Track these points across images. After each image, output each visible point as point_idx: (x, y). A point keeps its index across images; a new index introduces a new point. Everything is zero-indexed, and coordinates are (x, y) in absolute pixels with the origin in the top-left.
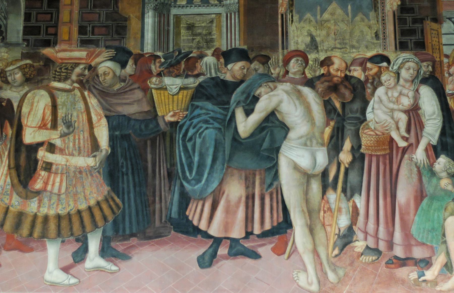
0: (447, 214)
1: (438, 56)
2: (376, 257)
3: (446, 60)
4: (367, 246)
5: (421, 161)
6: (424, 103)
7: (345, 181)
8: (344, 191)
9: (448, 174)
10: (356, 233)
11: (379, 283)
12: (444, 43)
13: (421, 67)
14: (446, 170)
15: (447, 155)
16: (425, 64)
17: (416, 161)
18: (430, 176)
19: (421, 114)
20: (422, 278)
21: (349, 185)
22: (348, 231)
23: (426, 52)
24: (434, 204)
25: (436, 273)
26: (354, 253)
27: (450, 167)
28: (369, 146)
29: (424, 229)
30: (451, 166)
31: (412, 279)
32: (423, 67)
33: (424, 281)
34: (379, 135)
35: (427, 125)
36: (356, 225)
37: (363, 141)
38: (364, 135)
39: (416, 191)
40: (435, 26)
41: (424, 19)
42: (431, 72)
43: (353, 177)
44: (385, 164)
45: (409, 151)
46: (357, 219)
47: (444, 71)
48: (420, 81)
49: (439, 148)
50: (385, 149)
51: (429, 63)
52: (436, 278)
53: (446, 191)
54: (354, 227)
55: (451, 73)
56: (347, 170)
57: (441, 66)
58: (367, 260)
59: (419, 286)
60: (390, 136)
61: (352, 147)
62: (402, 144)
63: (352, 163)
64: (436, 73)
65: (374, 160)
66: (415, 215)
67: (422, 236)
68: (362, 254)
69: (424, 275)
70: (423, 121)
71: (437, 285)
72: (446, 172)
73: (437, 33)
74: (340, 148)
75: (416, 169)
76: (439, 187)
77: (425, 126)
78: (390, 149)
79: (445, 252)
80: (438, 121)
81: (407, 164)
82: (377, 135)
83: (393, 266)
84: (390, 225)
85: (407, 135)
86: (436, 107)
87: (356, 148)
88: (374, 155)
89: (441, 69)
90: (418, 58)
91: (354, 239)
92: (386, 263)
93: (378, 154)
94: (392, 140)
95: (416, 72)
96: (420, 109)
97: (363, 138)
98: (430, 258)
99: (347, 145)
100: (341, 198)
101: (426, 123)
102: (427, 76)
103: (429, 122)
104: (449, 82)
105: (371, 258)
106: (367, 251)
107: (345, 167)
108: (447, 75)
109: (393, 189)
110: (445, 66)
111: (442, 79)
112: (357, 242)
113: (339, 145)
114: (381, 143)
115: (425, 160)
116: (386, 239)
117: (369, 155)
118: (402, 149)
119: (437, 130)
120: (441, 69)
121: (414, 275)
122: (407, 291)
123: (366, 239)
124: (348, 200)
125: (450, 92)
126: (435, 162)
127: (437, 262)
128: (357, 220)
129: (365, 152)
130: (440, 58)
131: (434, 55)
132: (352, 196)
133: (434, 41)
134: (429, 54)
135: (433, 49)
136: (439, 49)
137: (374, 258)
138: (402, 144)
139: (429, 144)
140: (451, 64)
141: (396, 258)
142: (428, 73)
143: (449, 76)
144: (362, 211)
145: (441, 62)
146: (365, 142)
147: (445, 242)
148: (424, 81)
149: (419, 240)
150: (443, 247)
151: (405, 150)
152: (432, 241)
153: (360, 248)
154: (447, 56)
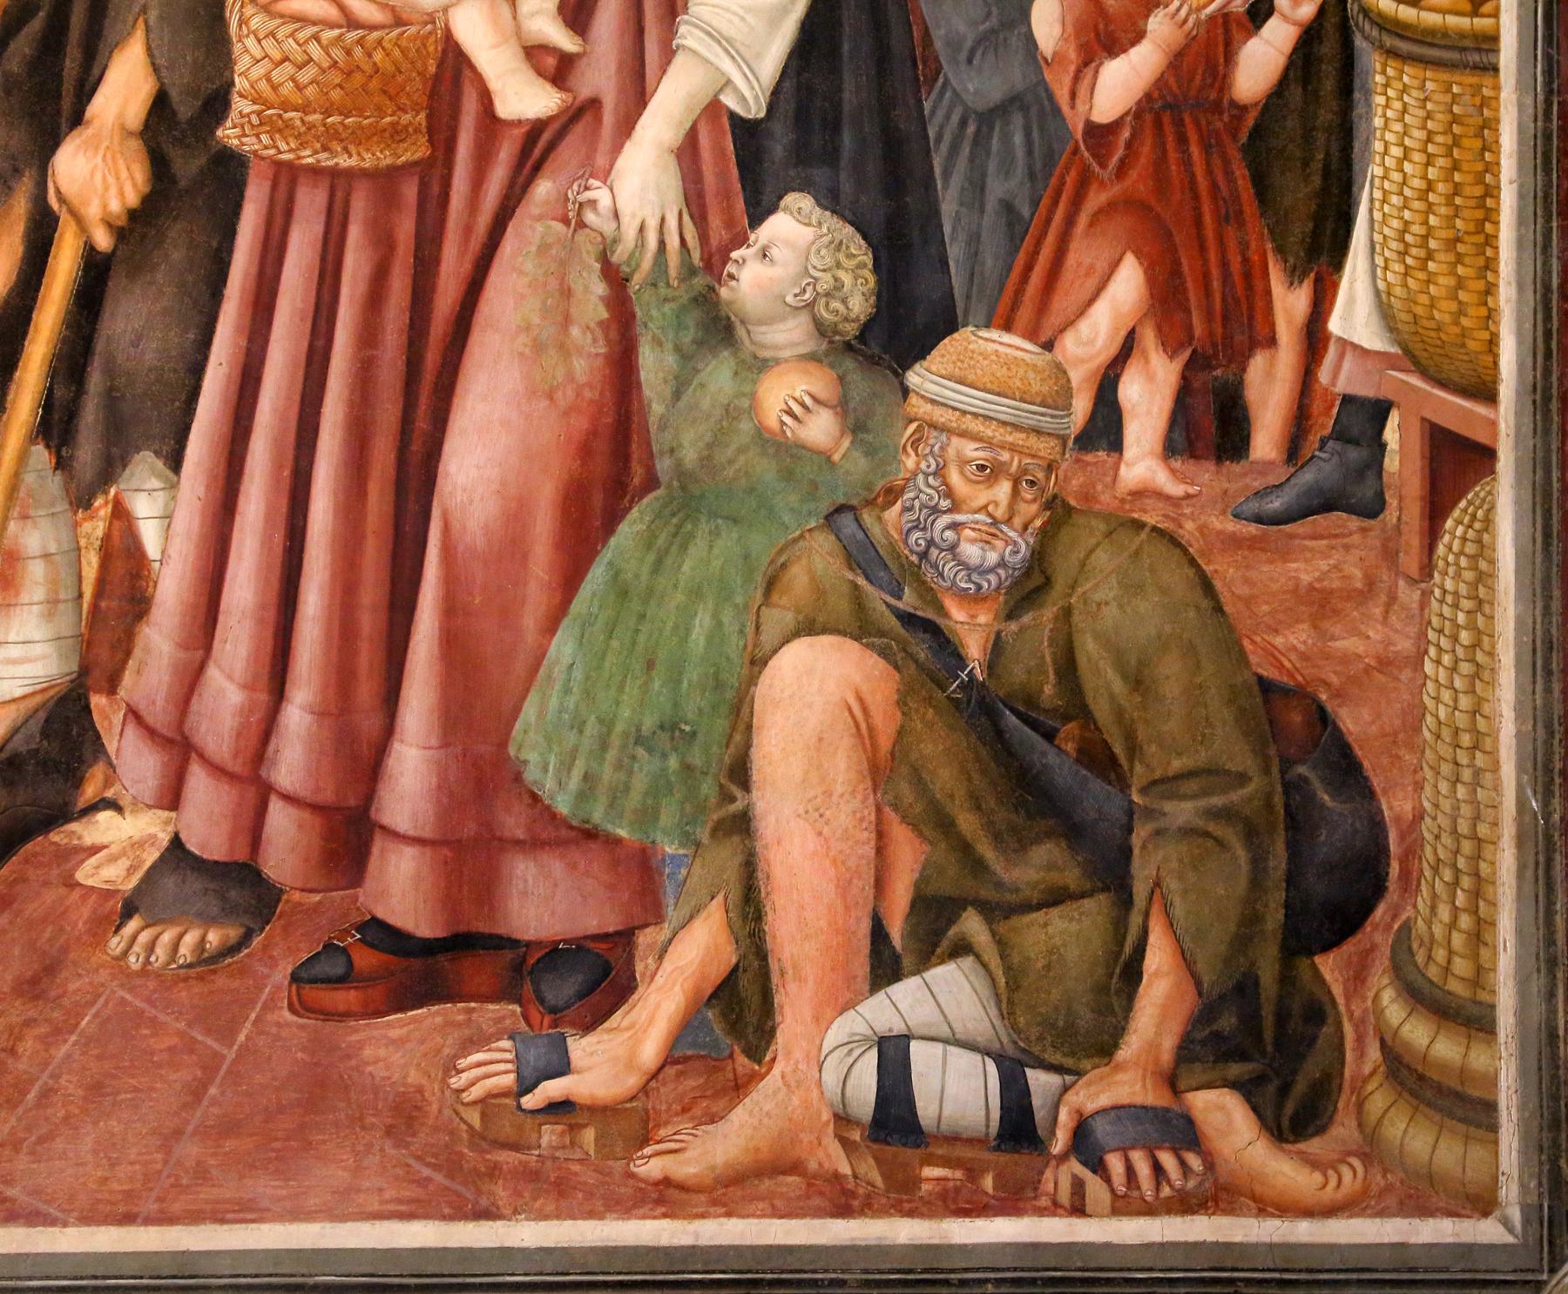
0: (778, 618)
2: (234, 933)
4: (176, 842)
5: (642, 229)
7: (73, 360)
8: (55, 426)
10: (111, 746)
11: (229, 1127)
14: (810, 305)
15: (831, 201)
17: (608, 228)
18: (699, 343)
20: (552, 1089)
21: (95, 381)
22: (45, 733)
24: (697, 549)
25: (650, 1051)
26: (76, 894)
27: (838, 285)
28: (286, 106)
29: (607, 724)
30: (847, 279)
31: (476, 1092)
33: (560, 1108)
34: (373, 28)
36: (112, 687)
37: (242, 63)
38: (255, 23)
39: (585, 451)
43: (136, 324)
44: (383, 245)
45: (569, 151)
46: (125, 646)
49: (779, 147)
50: (397, 134)
52: (644, 1089)
53: (787, 452)
54: (97, 701)
56: (96, 274)
58: (161, 953)
59: (515, 1147)
60: (448, 36)
61: (160, 104)
62: (524, 98)
63: (139, 225)
65: (310, 205)
66: (551, 626)
67: (586, 777)
68: (129, 911)
69: (563, 1068)
71: (645, 1141)
72: (804, 319)
74: (67, 103)
75: (600, 288)
76: (745, 426)
78: (431, 131)
79: (736, 894)
81: (543, 249)
82: (352, 22)
83: (345, 998)
84: (367, 691)
85: (565, 41)
87: (185, 109)
88: (315, 171)
91: (90, 791)
92: (295, 978)
93: (344, 162)
94: (454, 65)
97: (250, 42)
98: (624, 938)
99: (125, 87)
100: (29, 478)
105: (190, 939)
106: (170, 883)
107: (90, 251)
109: (422, 423)
112: (104, 816)
113: (58, 77)
114: (374, 84)
115: (672, 223)
116: (328, 796)
117: (279, 165)
118: (518, 132)
121: (489, 1070)
122: (424, 1182)
123: (172, 797)
124: (82, 501)
126: (741, 241)
127: (668, 965)
128: (128, 654)
129: (249, 145)
132: (109, 470)
137: (214, 938)
138: (524, 98)
141: (380, 933)
144: (172, 587)
146: (258, 71)
147: (742, 825)
149: (563, 806)
150: (726, 858)
151: (537, 146)
152: (646, 816)
153: (124, 863)
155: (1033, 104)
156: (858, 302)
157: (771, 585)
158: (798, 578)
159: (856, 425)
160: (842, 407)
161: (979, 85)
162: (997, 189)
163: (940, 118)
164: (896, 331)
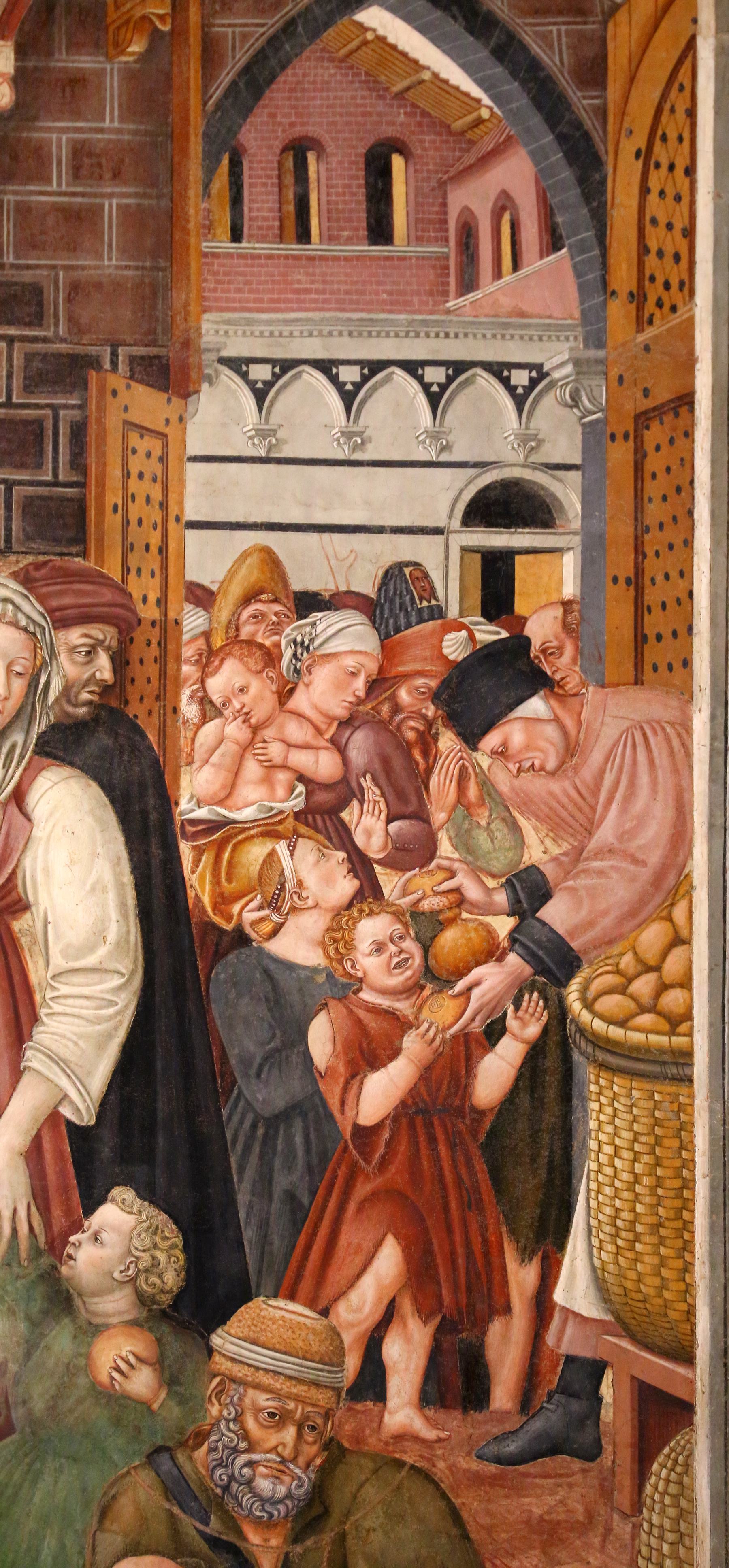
1: (152, 597)
3: (193, 621)
6: (47, 871)
9: (142, 1299)
12: (191, 515)
13: (53, 654)
14: (133, 1280)
15: (148, 1193)
16: (75, 636)
18: (45, 1313)
19: (24, 941)
23: (90, 564)
30: (162, 1257)
32: (63, 658)
35: (56, 1008)
40: (146, 403)
41: (94, 363)
42: (106, 690)
47: (178, 684)
48: (40, 736)
51: (97, 631)
55: (217, 699)
57: (162, 660)
64: (133, 694)
70: (34, 979)
72: (128, 1290)
73: (157, 452)
76: (82, 1381)
77: (43, 1012)
80: (117, 981)
86: (111, 898)
89: (163, 674)
90: (41, 599)
95: (19, 685)
96: (21, 906)
101: (49, 994)
102: (82, 711)
103: (64, 990)
104: (198, 756)
108: (189, 710)
110: (188, 652)
111: (162, 732)
115: (22, 1213)
119: (109, 1036)
120: (163, 674)
125: (202, 813)
126: (77, 1227)
130: (163, 602)
131: (135, 587)
133: (141, 500)
134: (104, 580)
135: (128, 548)
136: (163, 550)
139: (54, 1118)
140: (218, 642)
142: (85, 696)
143: (204, 719)
145: (168, 629)
148: (63, 743)
154: (202, 597)
155: (311, 1111)
156: (171, 1278)
157: (104, 1513)
158: (126, 1508)
159: (170, 1378)
160: (159, 1364)
161: (268, 1095)
162: (282, 1182)
163: (235, 1125)
164: (199, 1303)
